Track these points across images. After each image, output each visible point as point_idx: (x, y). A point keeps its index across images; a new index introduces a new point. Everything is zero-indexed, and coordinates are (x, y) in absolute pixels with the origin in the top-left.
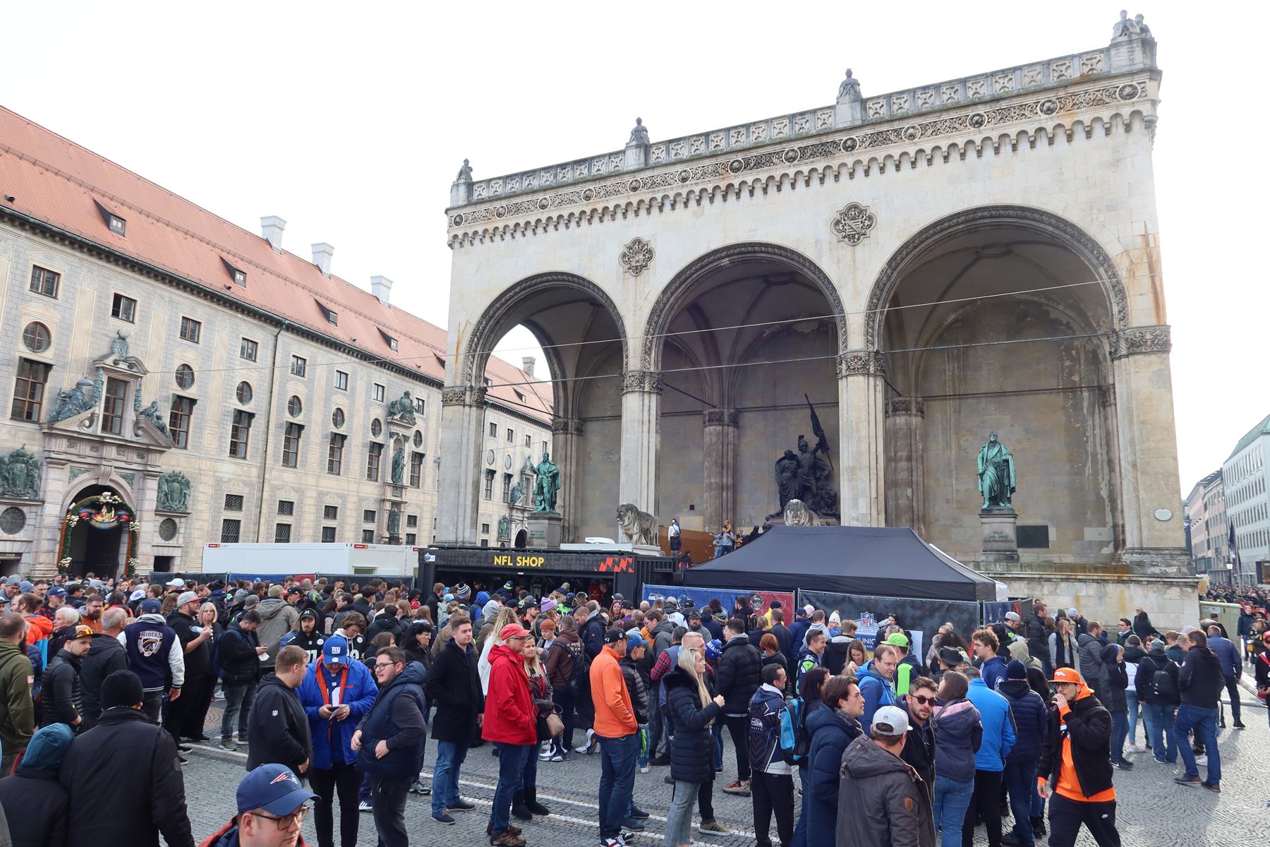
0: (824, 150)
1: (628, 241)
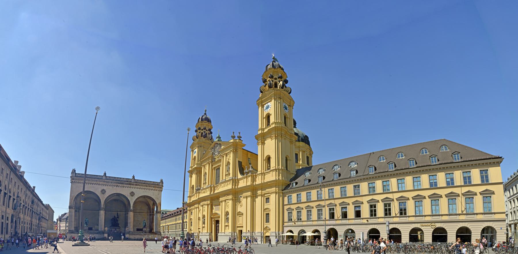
0: (130, 184)
1: (102, 189)
